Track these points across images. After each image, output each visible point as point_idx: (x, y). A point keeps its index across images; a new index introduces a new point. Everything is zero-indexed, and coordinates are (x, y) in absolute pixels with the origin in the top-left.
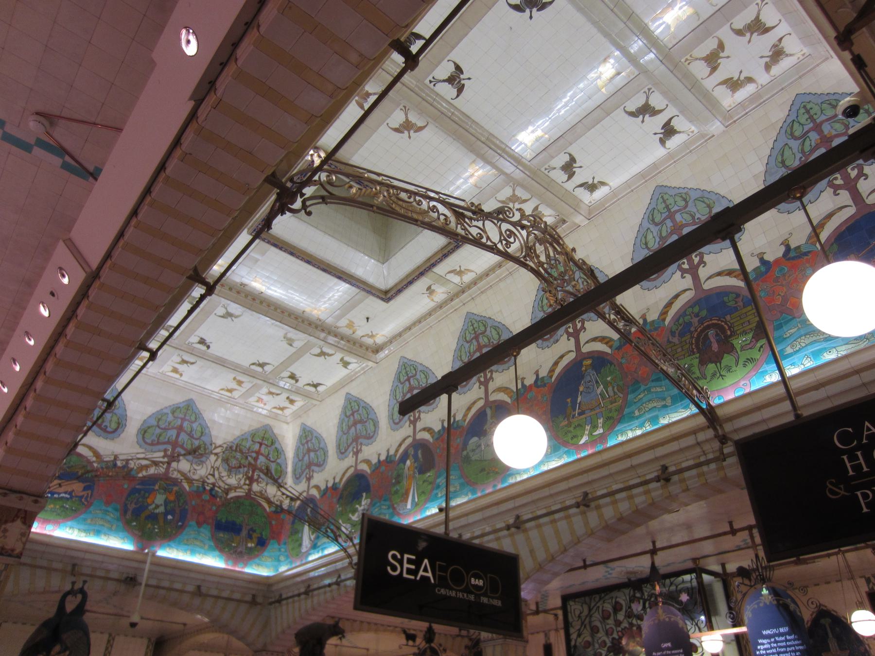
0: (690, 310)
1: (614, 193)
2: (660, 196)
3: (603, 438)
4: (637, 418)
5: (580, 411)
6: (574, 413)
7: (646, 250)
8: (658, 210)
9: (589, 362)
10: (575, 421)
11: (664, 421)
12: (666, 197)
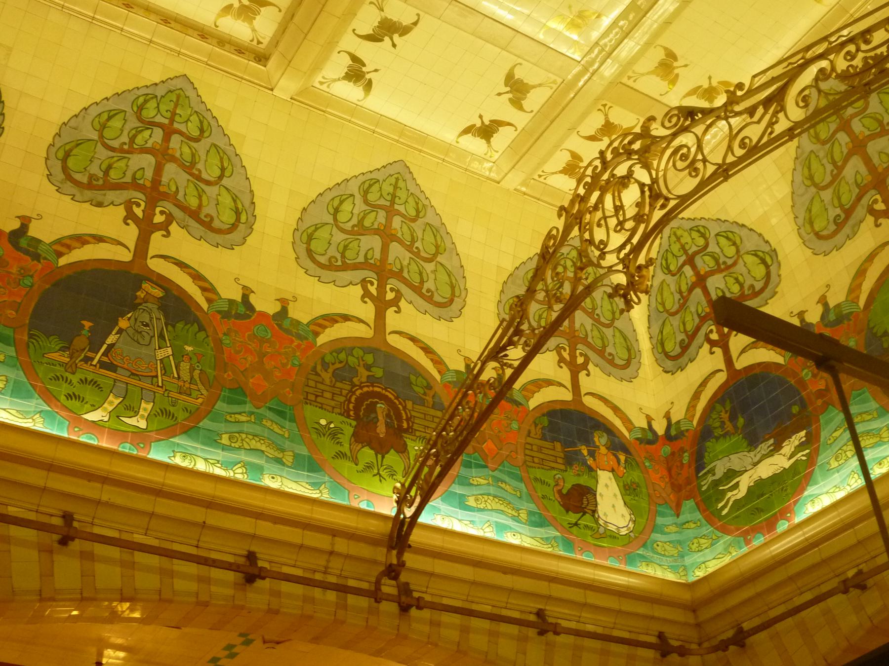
0: (361, 353)
1: (354, 110)
2: (396, 176)
3: (141, 437)
4: (224, 448)
5: (105, 359)
6: (90, 354)
7: (332, 217)
8: (381, 188)
9: (158, 293)
10: (87, 372)
12: (401, 184)
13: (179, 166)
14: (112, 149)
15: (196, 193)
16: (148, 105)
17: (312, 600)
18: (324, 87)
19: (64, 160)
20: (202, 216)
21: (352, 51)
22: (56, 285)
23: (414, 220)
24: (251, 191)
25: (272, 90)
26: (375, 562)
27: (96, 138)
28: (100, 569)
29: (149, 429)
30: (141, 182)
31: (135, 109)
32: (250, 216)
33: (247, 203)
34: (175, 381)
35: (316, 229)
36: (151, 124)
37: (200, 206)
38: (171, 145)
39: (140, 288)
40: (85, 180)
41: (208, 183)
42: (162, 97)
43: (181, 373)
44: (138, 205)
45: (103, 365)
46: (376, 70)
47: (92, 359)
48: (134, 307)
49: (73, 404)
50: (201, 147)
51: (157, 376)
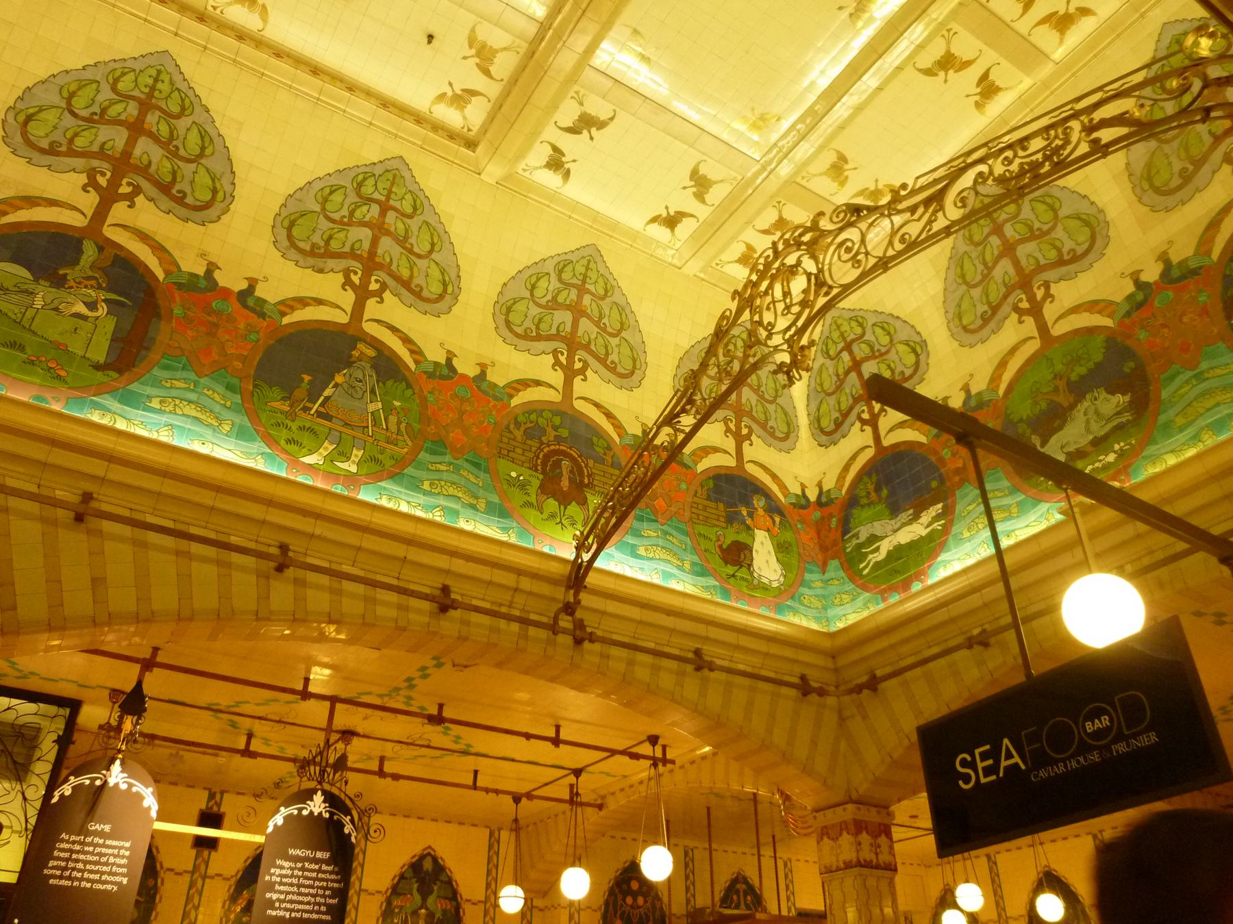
1: (552, 196)
3: (351, 480)
4: (425, 493)
5: (322, 410)
6: (309, 405)
9: (371, 353)
10: (306, 420)
11: (463, 524)
12: (592, 265)
13: (393, 239)
14: (333, 221)
15: (408, 265)
16: (366, 183)
17: (498, 631)
18: (527, 174)
19: (289, 229)
20: (413, 286)
21: (553, 142)
22: (280, 341)
23: (602, 298)
24: (458, 266)
25: (479, 174)
26: (553, 599)
27: (319, 210)
28: (310, 593)
29: (360, 473)
30: (359, 252)
31: (355, 185)
32: (456, 288)
33: (453, 276)
34: (384, 432)
35: (515, 303)
36: (369, 200)
37: (411, 277)
38: (387, 220)
39: (355, 348)
40: (308, 248)
41: (419, 256)
42: (380, 175)
43: (389, 425)
44: (356, 273)
45: (320, 415)
46: (574, 161)
47: (310, 409)
48: (349, 364)
49: (292, 448)
50: (414, 224)
51: (368, 427)
